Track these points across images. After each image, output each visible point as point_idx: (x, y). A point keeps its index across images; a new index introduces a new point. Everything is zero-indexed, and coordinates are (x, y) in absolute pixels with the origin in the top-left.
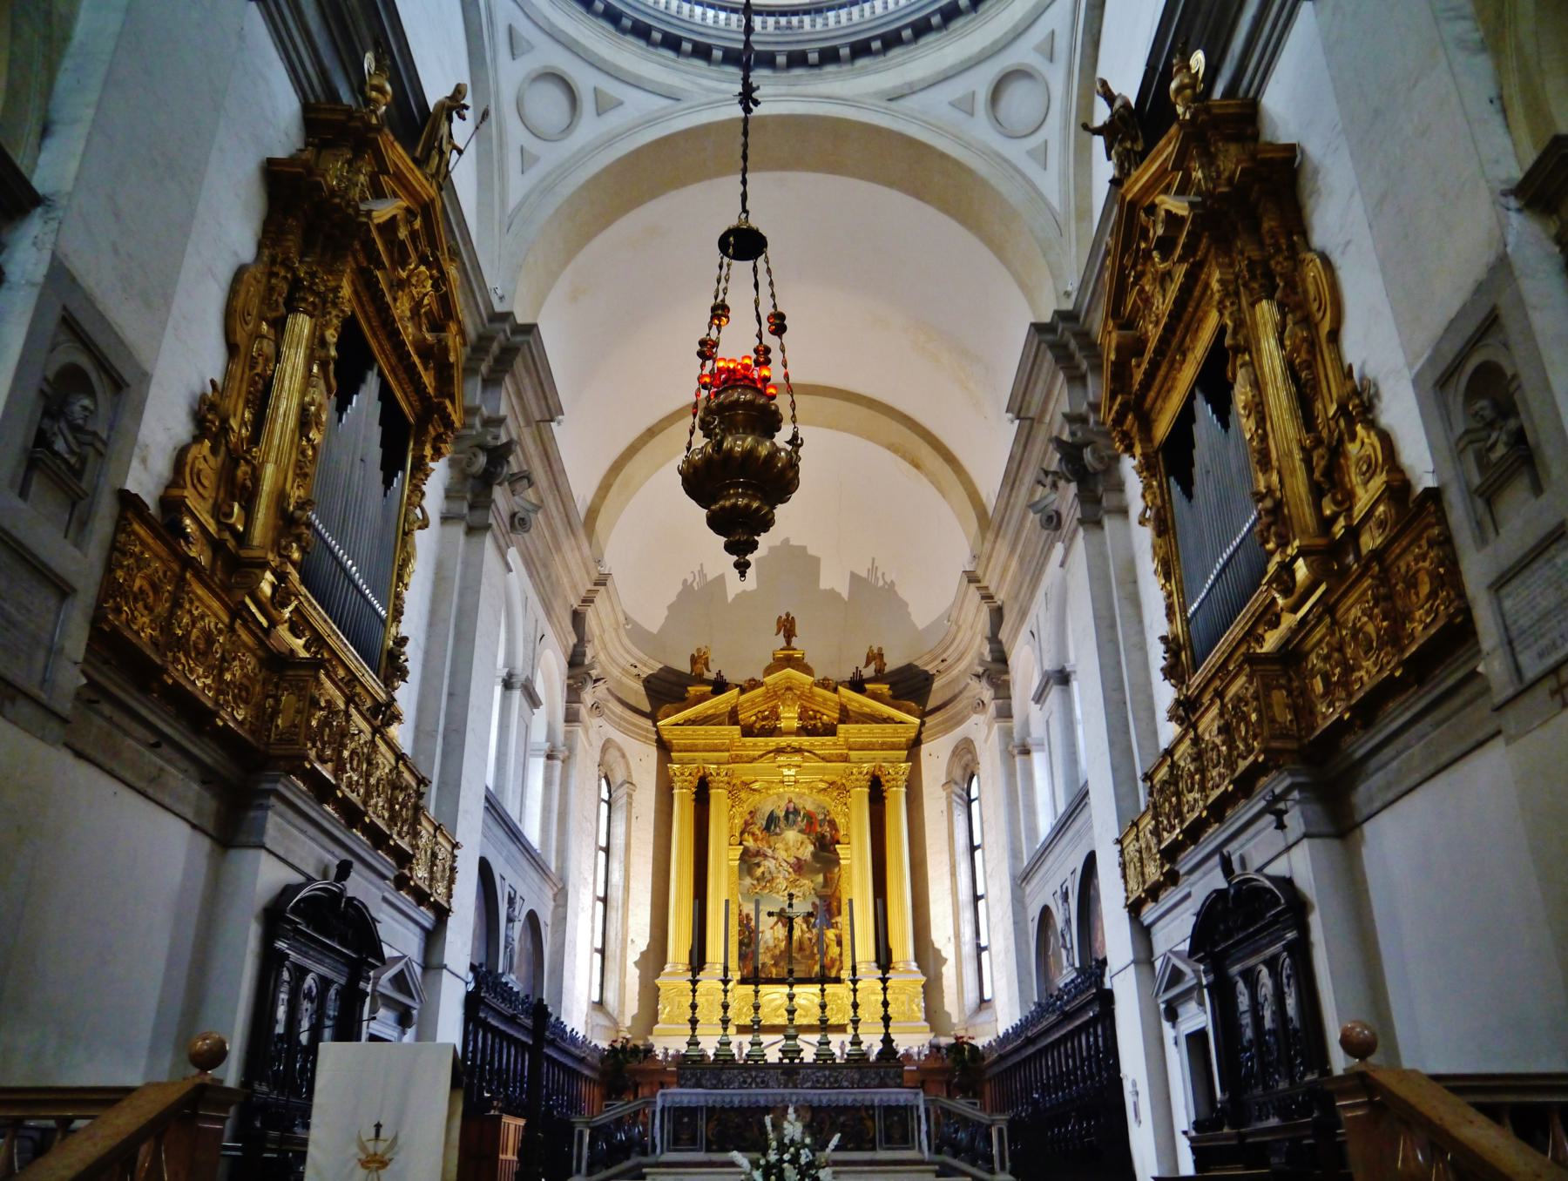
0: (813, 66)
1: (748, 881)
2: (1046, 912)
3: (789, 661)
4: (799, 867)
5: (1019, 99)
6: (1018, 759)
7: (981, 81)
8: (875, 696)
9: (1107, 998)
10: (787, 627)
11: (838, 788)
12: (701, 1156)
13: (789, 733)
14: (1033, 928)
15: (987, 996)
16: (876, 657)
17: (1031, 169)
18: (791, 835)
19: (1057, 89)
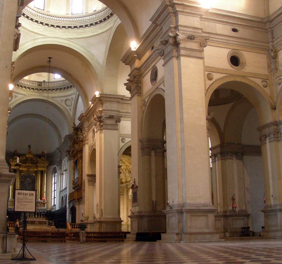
0: (43, 91)
1: (21, 186)
2: (63, 197)
3: (30, 153)
4: (29, 183)
5: (68, 102)
6: (62, 175)
7: (64, 99)
8: (43, 160)
9: (66, 211)
10: (30, 147)
11: (36, 172)
12: (30, 225)
13: (29, 163)
14: (61, 198)
15: (55, 204)
16: (43, 153)
17: (69, 111)
18: (28, 179)
19: (73, 104)
